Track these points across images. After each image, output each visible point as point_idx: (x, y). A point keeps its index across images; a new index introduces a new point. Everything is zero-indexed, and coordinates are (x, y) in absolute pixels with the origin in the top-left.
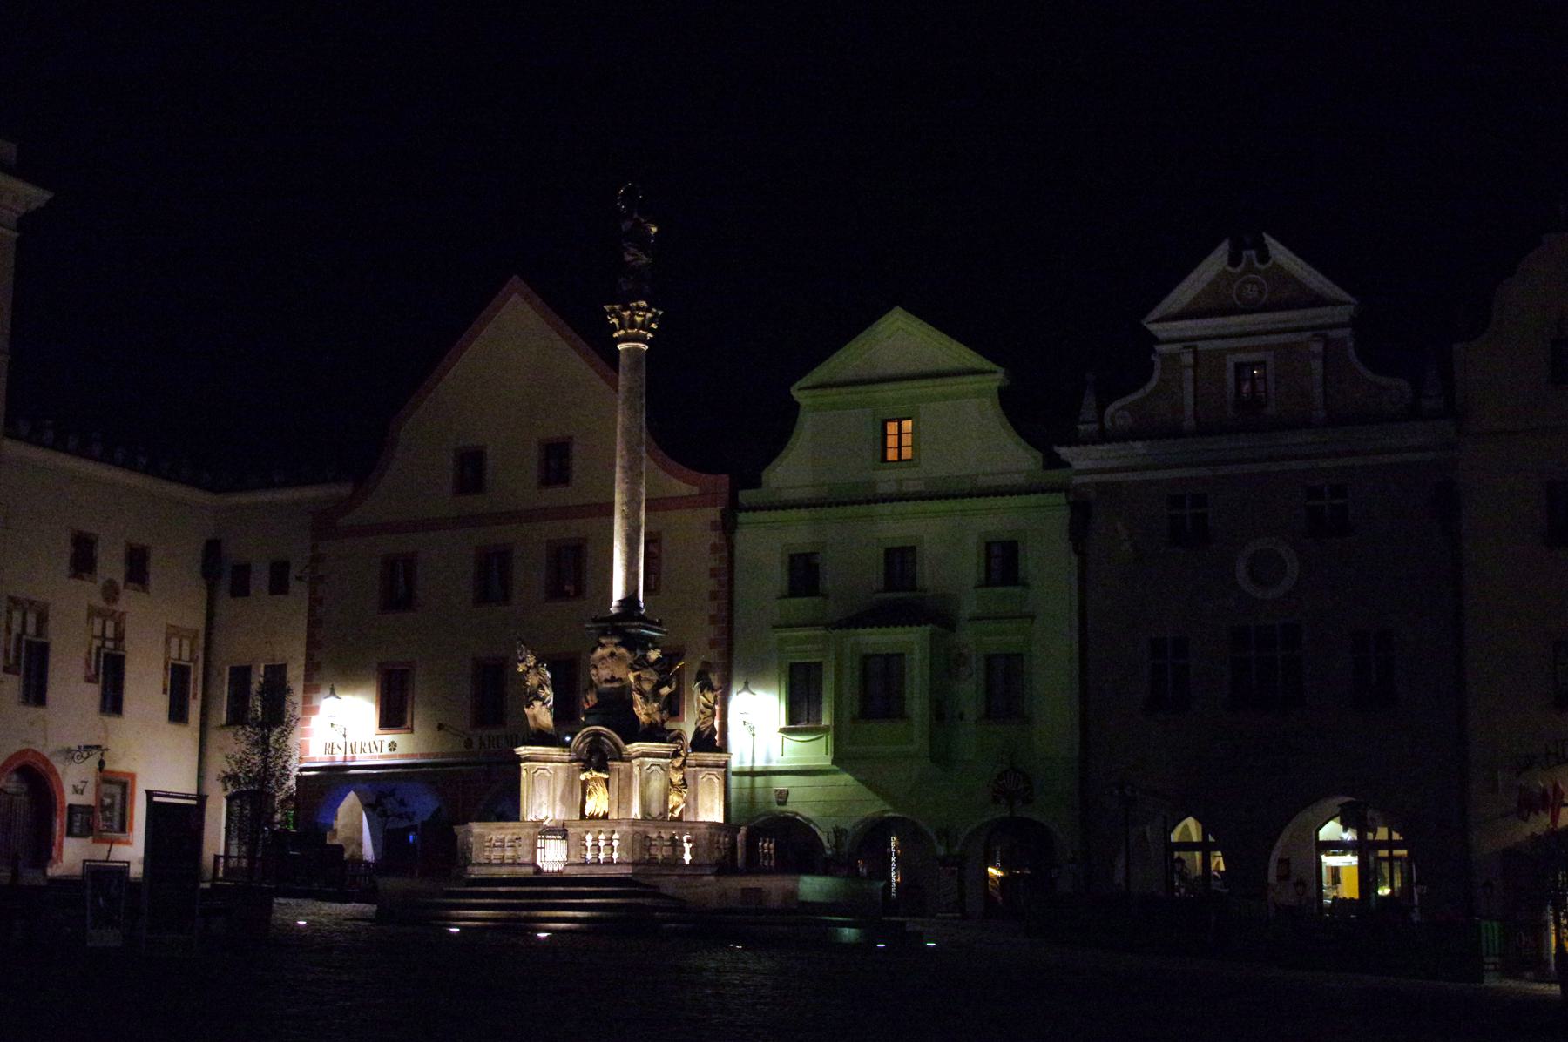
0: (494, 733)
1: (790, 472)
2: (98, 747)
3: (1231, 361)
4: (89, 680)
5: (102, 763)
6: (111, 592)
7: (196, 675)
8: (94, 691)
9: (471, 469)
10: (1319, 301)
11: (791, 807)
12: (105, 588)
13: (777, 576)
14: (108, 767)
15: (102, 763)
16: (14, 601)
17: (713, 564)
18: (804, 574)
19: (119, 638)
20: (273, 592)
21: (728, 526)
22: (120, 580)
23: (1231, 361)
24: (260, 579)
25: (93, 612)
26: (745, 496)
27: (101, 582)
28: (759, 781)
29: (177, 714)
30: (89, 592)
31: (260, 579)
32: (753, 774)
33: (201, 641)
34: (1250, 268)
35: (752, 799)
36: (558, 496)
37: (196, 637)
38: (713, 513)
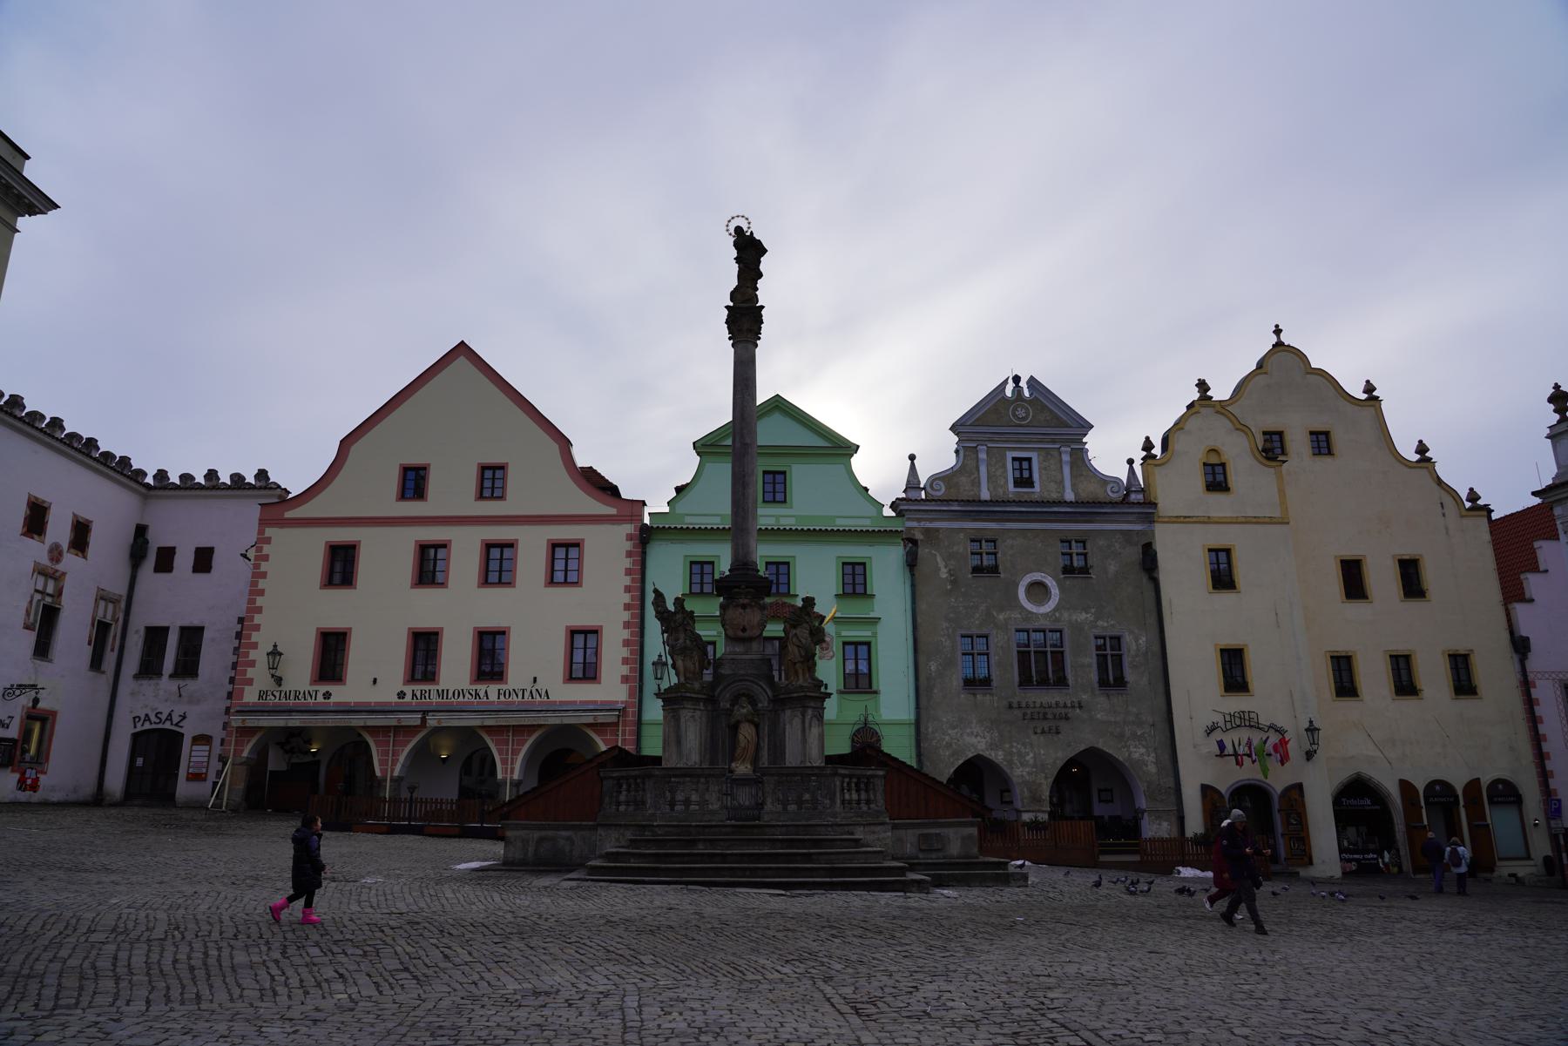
0: (426, 687)
2: (33, 687)
3: (1010, 455)
4: (27, 627)
5: (36, 701)
6: (56, 554)
7: (116, 630)
8: (31, 637)
9: (414, 482)
12: (51, 551)
14: (40, 705)
15: (36, 701)
19: (59, 593)
22: (65, 546)
23: (1010, 455)
24: (185, 560)
25: (41, 571)
27: (47, 547)
29: (96, 663)
30: (37, 551)
31: (185, 560)
33: (123, 605)
38: (629, 528)
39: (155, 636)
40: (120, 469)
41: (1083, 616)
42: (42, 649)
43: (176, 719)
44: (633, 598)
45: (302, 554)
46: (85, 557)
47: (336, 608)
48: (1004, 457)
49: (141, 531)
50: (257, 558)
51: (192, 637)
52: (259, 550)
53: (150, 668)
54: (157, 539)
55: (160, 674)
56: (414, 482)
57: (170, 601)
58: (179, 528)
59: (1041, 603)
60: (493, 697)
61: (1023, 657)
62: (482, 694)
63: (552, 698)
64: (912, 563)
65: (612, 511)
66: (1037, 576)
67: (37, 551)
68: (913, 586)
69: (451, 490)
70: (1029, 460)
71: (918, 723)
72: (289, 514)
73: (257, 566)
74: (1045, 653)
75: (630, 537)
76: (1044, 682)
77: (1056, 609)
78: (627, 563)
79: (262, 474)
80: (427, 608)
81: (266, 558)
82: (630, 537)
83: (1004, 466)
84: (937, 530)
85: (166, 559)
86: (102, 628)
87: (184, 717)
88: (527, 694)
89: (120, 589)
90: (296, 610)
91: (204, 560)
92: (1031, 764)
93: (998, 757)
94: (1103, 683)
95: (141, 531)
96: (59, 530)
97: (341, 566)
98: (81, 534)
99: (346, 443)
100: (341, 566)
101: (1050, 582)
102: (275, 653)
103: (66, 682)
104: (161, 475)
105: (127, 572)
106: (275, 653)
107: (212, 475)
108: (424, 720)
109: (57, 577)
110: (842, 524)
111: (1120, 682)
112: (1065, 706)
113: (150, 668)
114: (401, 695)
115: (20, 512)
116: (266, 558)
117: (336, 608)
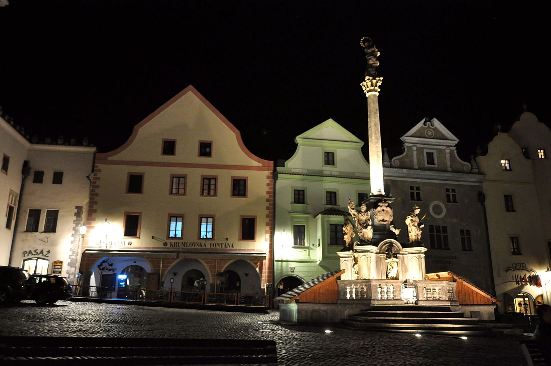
1: (294, 163)
3: (425, 151)
9: (169, 147)
10: (446, 139)
11: (295, 274)
13: (290, 197)
17: (268, 190)
18: (300, 196)
20: (54, 182)
21: (275, 176)
23: (425, 151)
24: (48, 177)
26: (279, 169)
28: (284, 264)
29: (8, 226)
31: (48, 177)
32: (282, 261)
33: (18, 198)
34: (429, 127)
35: (282, 270)
36: (205, 160)
37: (17, 197)
38: (267, 173)
41: (455, 220)
43: (45, 253)
44: (270, 204)
46: (7, 174)
48: (423, 152)
50: (94, 178)
52: (95, 175)
53: (33, 227)
55: (36, 230)
59: (439, 214)
60: (208, 246)
62: (203, 245)
63: (235, 248)
65: (261, 165)
66: (437, 202)
69: (187, 151)
70: (432, 153)
72: (109, 159)
73: (95, 182)
74: (440, 235)
75: (268, 177)
76: (440, 248)
77: (445, 217)
81: (99, 179)
82: (268, 177)
83: (423, 155)
84: (397, 181)
86: (11, 209)
87: (49, 252)
88: (223, 245)
94: (464, 249)
101: (442, 205)
108: (178, 255)
111: (470, 250)
112: (449, 258)
114: (165, 244)
116: (99, 179)
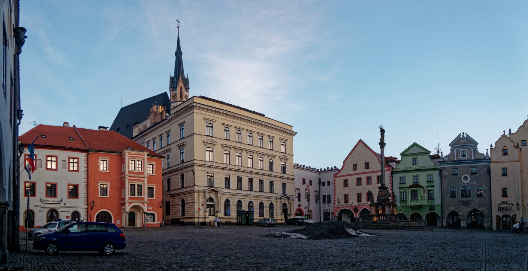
6: (308, 186)
9: (355, 167)
16: (296, 189)
24: (326, 184)
29: (317, 202)
30: (305, 186)
31: (326, 184)
38: (390, 172)
39: (324, 197)
40: (314, 170)
42: (309, 201)
45: (340, 181)
47: (346, 191)
49: (320, 179)
51: (329, 196)
54: (322, 181)
56: (355, 167)
57: (325, 191)
58: (325, 178)
61: (462, 191)
64: (441, 174)
67: (305, 186)
68: (441, 179)
69: (361, 168)
71: (442, 206)
78: (390, 178)
79: (335, 167)
80: (359, 189)
85: (324, 183)
89: (318, 190)
90: (340, 192)
91: (329, 183)
92: (463, 211)
93: (457, 211)
95: (320, 179)
96: (307, 183)
97: (346, 183)
98: (311, 182)
99: (344, 162)
100: (346, 183)
102: (338, 199)
103: (313, 206)
104: (321, 169)
105: (318, 187)
106: (338, 199)
107: (328, 168)
109: (308, 190)
110: (428, 167)
113: (324, 202)
115: (302, 181)
117: (346, 191)
